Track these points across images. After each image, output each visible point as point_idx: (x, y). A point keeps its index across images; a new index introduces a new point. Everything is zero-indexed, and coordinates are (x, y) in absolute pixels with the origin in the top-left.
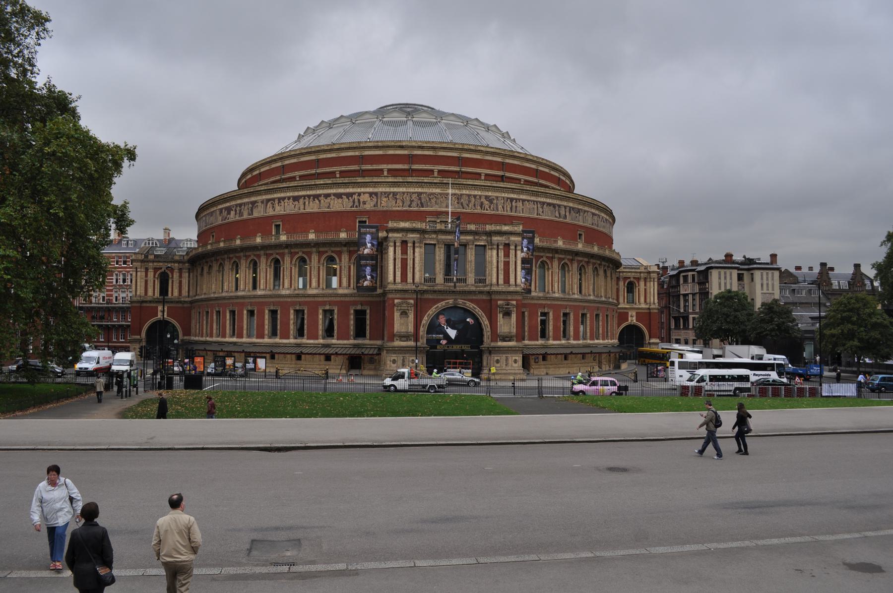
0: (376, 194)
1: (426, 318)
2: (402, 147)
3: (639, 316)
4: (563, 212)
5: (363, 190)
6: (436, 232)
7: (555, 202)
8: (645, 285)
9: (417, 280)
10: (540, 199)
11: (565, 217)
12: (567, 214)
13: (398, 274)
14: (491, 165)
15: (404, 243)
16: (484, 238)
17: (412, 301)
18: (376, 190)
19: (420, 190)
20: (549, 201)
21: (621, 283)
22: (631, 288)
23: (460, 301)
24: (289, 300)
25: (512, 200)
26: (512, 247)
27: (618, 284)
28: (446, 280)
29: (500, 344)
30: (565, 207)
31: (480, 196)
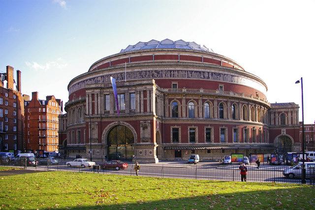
0: (103, 76)
1: (104, 131)
2: (125, 55)
3: (287, 131)
4: (206, 75)
5: (98, 75)
6: (108, 88)
7: (200, 70)
8: (292, 115)
9: (99, 113)
10: (189, 69)
11: (209, 77)
12: (210, 76)
13: (91, 110)
14: (171, 57)
15: (93, 95)
16: (134, 89)
17: (97, 123)
18: (103, 74)
19: (121, 71)
20: (195, 70)
21: (277, 115)
22: (283, 117)
23: (121, 122)
24: (76, 127)
25: (171, 71)
26: (148, 92)
27: (275, 116)
28: (115, 112)
29: (141, 143)
30: (208, 73)
31: (152, 71)
